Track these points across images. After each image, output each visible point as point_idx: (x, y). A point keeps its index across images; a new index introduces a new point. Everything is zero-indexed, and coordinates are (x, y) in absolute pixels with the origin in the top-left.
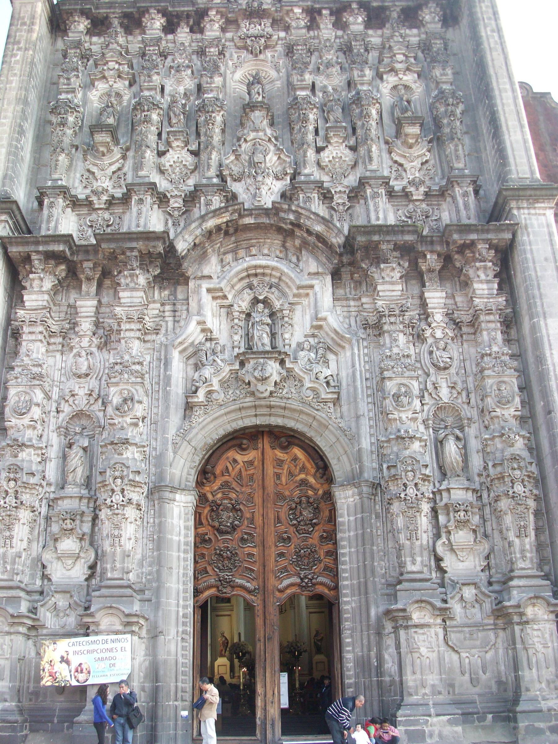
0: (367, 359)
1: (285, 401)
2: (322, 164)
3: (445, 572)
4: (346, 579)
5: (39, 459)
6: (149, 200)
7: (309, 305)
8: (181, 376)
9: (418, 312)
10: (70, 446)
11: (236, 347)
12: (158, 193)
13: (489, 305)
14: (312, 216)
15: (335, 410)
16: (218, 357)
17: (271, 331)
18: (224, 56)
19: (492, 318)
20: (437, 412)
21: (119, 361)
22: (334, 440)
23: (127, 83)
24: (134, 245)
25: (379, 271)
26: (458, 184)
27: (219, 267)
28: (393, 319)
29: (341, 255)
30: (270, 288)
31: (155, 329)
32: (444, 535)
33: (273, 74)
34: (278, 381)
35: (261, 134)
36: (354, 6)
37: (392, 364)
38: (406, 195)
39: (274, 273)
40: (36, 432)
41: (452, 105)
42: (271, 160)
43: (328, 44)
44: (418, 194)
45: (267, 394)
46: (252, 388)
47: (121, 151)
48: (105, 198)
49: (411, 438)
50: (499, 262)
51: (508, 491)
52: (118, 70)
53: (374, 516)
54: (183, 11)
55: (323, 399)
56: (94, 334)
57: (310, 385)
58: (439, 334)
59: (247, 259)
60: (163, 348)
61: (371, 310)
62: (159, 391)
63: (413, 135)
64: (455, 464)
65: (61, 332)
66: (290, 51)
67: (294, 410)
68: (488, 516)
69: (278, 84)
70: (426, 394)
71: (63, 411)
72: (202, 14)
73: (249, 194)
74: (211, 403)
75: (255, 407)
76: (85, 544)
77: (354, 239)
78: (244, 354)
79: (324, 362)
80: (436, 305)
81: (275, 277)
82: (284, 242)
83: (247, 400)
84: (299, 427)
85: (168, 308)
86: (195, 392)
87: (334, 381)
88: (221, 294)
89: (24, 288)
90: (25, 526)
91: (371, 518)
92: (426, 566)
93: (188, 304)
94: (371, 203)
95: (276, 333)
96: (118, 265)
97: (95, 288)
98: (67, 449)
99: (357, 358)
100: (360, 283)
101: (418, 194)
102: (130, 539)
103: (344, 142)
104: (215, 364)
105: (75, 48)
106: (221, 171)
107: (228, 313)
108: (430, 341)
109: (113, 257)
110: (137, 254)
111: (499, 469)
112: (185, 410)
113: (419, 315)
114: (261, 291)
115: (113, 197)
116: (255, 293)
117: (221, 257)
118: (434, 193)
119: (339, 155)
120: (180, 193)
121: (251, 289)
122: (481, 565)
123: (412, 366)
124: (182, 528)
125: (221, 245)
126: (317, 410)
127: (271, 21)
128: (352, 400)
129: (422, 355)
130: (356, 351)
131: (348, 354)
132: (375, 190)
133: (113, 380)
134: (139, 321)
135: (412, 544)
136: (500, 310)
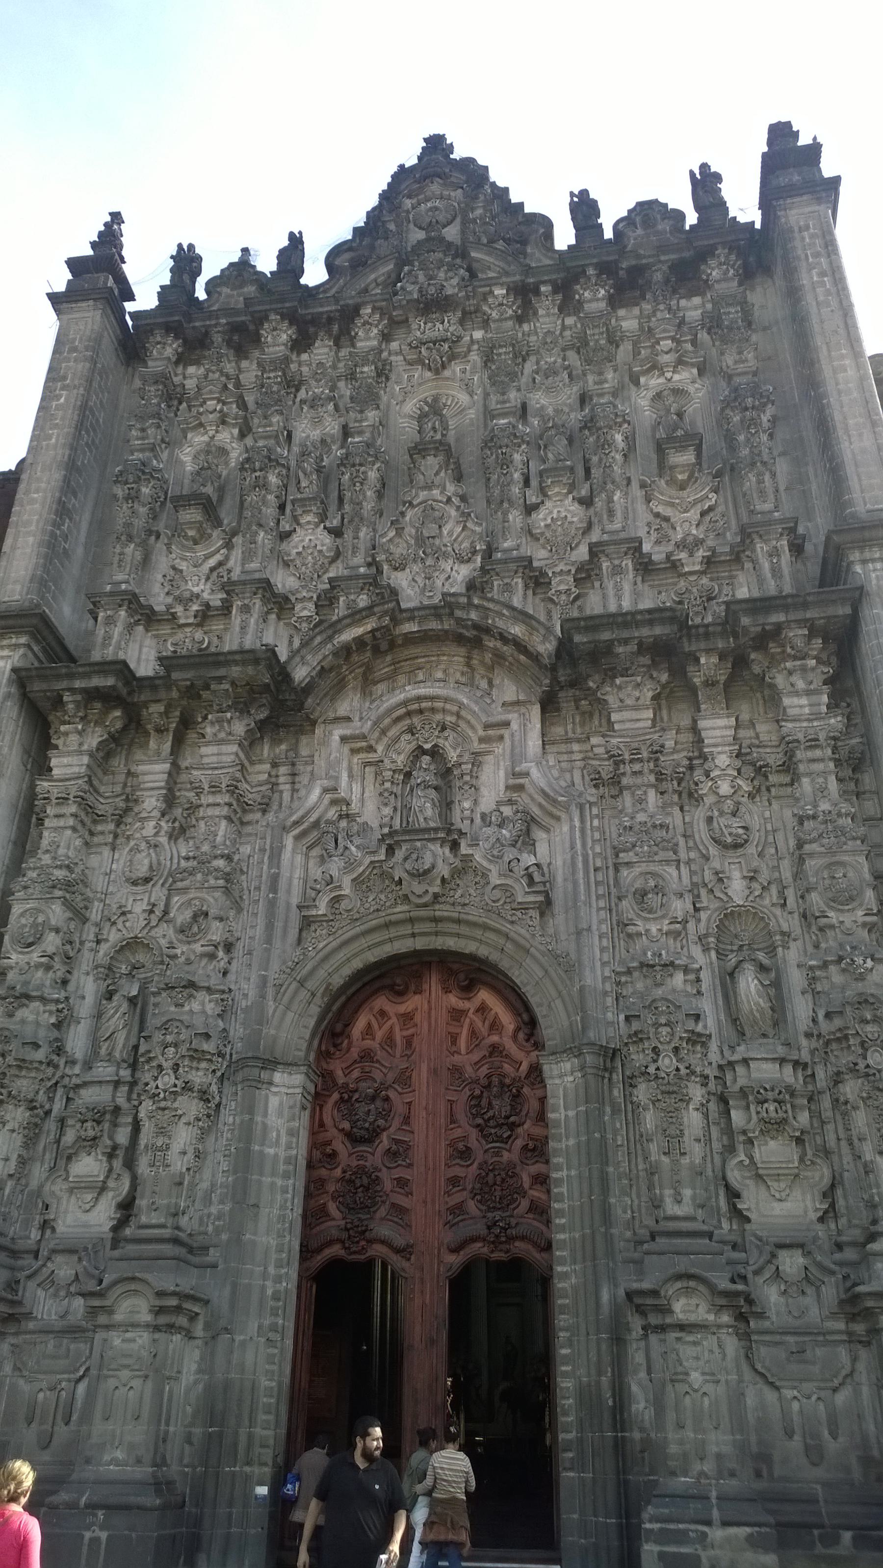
0: (597, 836)
1: (459, 908)
2: (534, 532)
3: (748, 1220)
4: (562, 1229)
5: (53, 1020)
6: (257, 605)
7: (503, 755)
8: (297, 876)
9: (685, 754)
10: (109, 995)
12: (274, 595)
13: (810, 731)
14: (505, 611)
18: (387, 379)
19: (818, 753)
20: (727, 923)
21: (191, 854)
22: (540, 974)
23: (236, 431)
24: (222, 672)
26: (761, 536)
28: (637, 767)
30: (444, 728)
32: (740, 1148)
33: (463, 398)
35: (436, 492)
36: (591, 271)
38: (673, 566)
40: (50, 974)
41: (753, 408)
42: (450, 533)
43: (549, 340)
44: (692, 563)
45: (427, 899)
46: (405, 889)
47: (223, 535)
48: (195, 607)
49: (665, 965)
50: (834, 660)
51: (856, 1064)
52: (221, 411)
53: (608, 1110)
54: (322, 313)
55: (519, 903)
56: (163, 815)
57: (498, 882)
58: (725, 788)
60: (269, 832)
63: (683, 466)
64: (758, 1015)
65: (113, 815)
66: (488, 359)
67: (474, 925)
68: (828, 1114)
69: (472, 414)
70: (703, 892)
71: (107, 940)
72: (350, 314)
73: (417, 589)
75: (411, 920)
76: (117, 1164)
77: (571, 640)
80: (719, 740)
82: (469, 658)
83: (399, 908)
84: (483, 951)
85: (283, 770)
88: (364, 744)
89: (56, 747)
90: (15, 1135)
91: (601, 1114)
92: (702, 1206)
94: (610, 585)
97: (169, 744)
98: (104, 1002)
99: (578, 834)
100: (591, 715)
101: (692, 563)
102: (185, 1153)
103: (570, 492)
104: (347, 852)
105: (156, 382)
106: (373, 557)
107: (376, 774)
108: (709, 800)
109: (192, 692)
111: (838, 1022)
112: (301, 930)
113: (690, 759)
115: (207, 606)
116: (418, 739)
118: (723, 558)
119: (563, 515)
120: (311, 594)
122: (817, 1210)
123: (668, 841)
124: (283, 1133)
126: (512, 922)
127: (459, 314)
129: (695, 826)
130: (577, 823)
131: (566, 828)
132: (616, 562)
133: (180, 885)
134: (228, 791)
135: (675, 1162)
136: (835, 739)
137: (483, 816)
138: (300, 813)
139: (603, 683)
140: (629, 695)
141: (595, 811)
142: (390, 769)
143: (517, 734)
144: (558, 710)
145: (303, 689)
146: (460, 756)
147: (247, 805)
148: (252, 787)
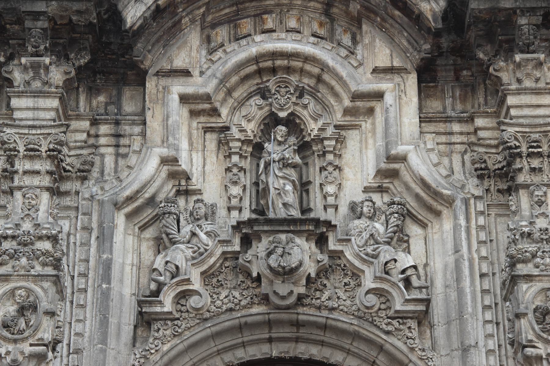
1: (325, 313)
8: (129, 261)
11: (234, 208)
15: (421, 333)
16: (200, 227)
17: (301, 177)
21: (9, 232)
25: (511, 67)
27: (204, 52)
28: (535, 163)
29: (438, 34)
30: (301, 96)
31: (79, 171)
34: (313, 275)
37: (532, 248)
39: (308, 67)
45: (292, 300)
46: (265, 288)
55: (397, 312)
57: (373, 286)
59: (258, 38)
60: (96, 207)
61: (493, 142)
62: (85, 290)
74: (185, 315)
75: (269, 324)
78: (250, 222)
79: (400, 240)
81: (310, 75)
83: (255, 310)
85: (104, 129)
86: (156, 293)
87: (419, 277)
88: (207, 106)
93: (144, 123)
95: (309, 183)
96: (8, 44)
99: (464, 235)
100: (474, 90)
104: (195, 240)
107: (220, 142)
110: (46, 25)
112: (135, 327)
114: (282, 101)
116: (271, 105)
117: (206, 32)
121: (264, 97)
125: (208, 9)
126: (388, 333)
128: (453, 315)
130: (462, 222)
134: (49, 157)
137: (353, 207)
138: (135, 187)
139: (495, 56)
140: (528, 75)
142: (239, 140)
143: (392, 110)
144: (434, 79)
145: (134, 31)
146: (321, 130)
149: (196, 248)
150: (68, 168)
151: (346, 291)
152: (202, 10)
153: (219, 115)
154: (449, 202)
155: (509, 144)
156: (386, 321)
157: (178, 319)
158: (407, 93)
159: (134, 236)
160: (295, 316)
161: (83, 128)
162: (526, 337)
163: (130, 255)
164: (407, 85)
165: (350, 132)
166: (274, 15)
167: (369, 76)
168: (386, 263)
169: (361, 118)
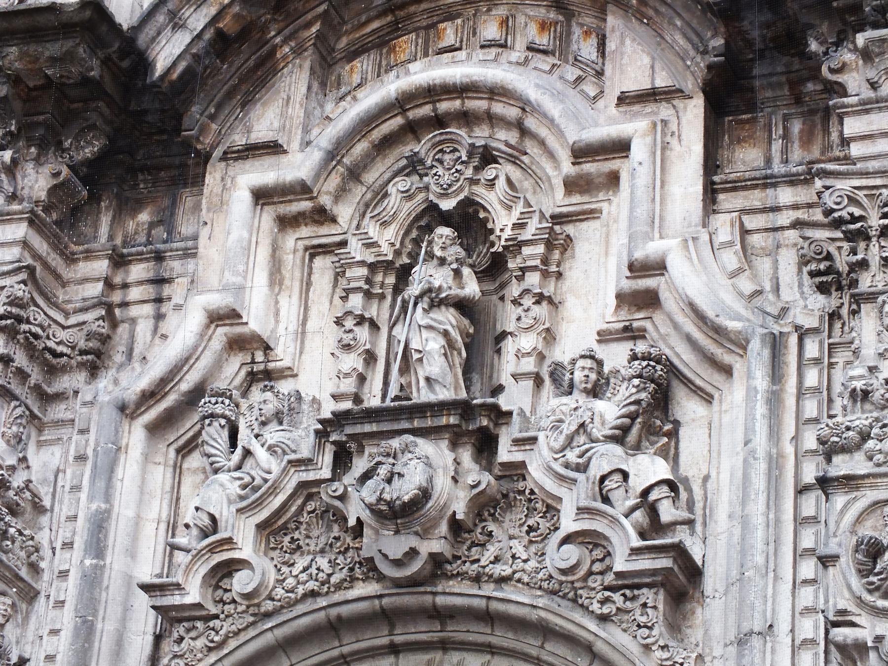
1: (489, 589)
31: (83, 352)
34: (460, 516)
39: (498, 108)
45: (415, 567)
55: (619, 575)
85: (138, 271)
88: (305, 205)
99: (761, 409)
116: (427, 188)
126: (604, 619)
141: (812, 349)
142: (362, 263)
145: (172, 83)
146: (519, 226)
147: (56, 355)
148: (67, 315)
149: (247, 479)
150: (60, 349)
151: (531, 542)
152: (314, 29)
153: (334, 220)
154: (740, 344)
155: (836, 215)
156: (599, 596)
157: (216, 617)
158: (683, 137)
159: (165, 465)
160: (428, 599)
161: (96, 274)
162: (835, 605)
163: (156, 504)
164: (684, 121)
165: (584, 225)
166: (459, 21)
167: (613, 111)
168: (603, 479)
169: (601, 196)
